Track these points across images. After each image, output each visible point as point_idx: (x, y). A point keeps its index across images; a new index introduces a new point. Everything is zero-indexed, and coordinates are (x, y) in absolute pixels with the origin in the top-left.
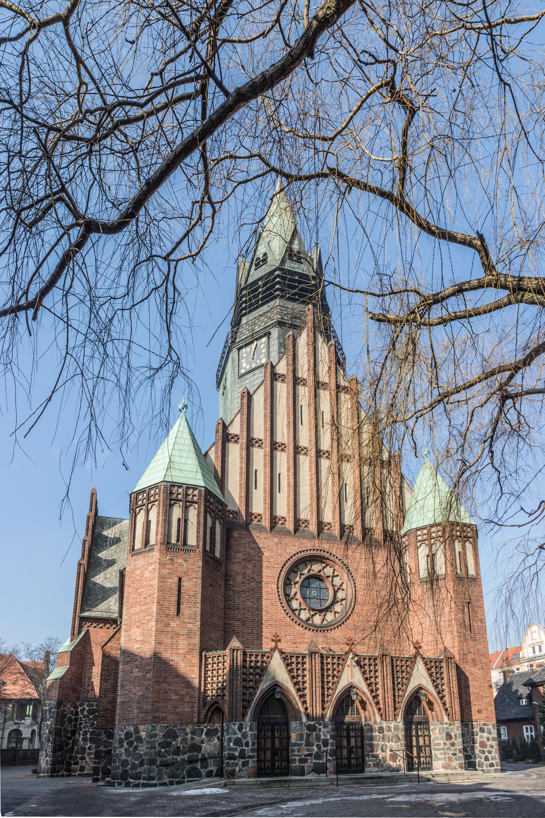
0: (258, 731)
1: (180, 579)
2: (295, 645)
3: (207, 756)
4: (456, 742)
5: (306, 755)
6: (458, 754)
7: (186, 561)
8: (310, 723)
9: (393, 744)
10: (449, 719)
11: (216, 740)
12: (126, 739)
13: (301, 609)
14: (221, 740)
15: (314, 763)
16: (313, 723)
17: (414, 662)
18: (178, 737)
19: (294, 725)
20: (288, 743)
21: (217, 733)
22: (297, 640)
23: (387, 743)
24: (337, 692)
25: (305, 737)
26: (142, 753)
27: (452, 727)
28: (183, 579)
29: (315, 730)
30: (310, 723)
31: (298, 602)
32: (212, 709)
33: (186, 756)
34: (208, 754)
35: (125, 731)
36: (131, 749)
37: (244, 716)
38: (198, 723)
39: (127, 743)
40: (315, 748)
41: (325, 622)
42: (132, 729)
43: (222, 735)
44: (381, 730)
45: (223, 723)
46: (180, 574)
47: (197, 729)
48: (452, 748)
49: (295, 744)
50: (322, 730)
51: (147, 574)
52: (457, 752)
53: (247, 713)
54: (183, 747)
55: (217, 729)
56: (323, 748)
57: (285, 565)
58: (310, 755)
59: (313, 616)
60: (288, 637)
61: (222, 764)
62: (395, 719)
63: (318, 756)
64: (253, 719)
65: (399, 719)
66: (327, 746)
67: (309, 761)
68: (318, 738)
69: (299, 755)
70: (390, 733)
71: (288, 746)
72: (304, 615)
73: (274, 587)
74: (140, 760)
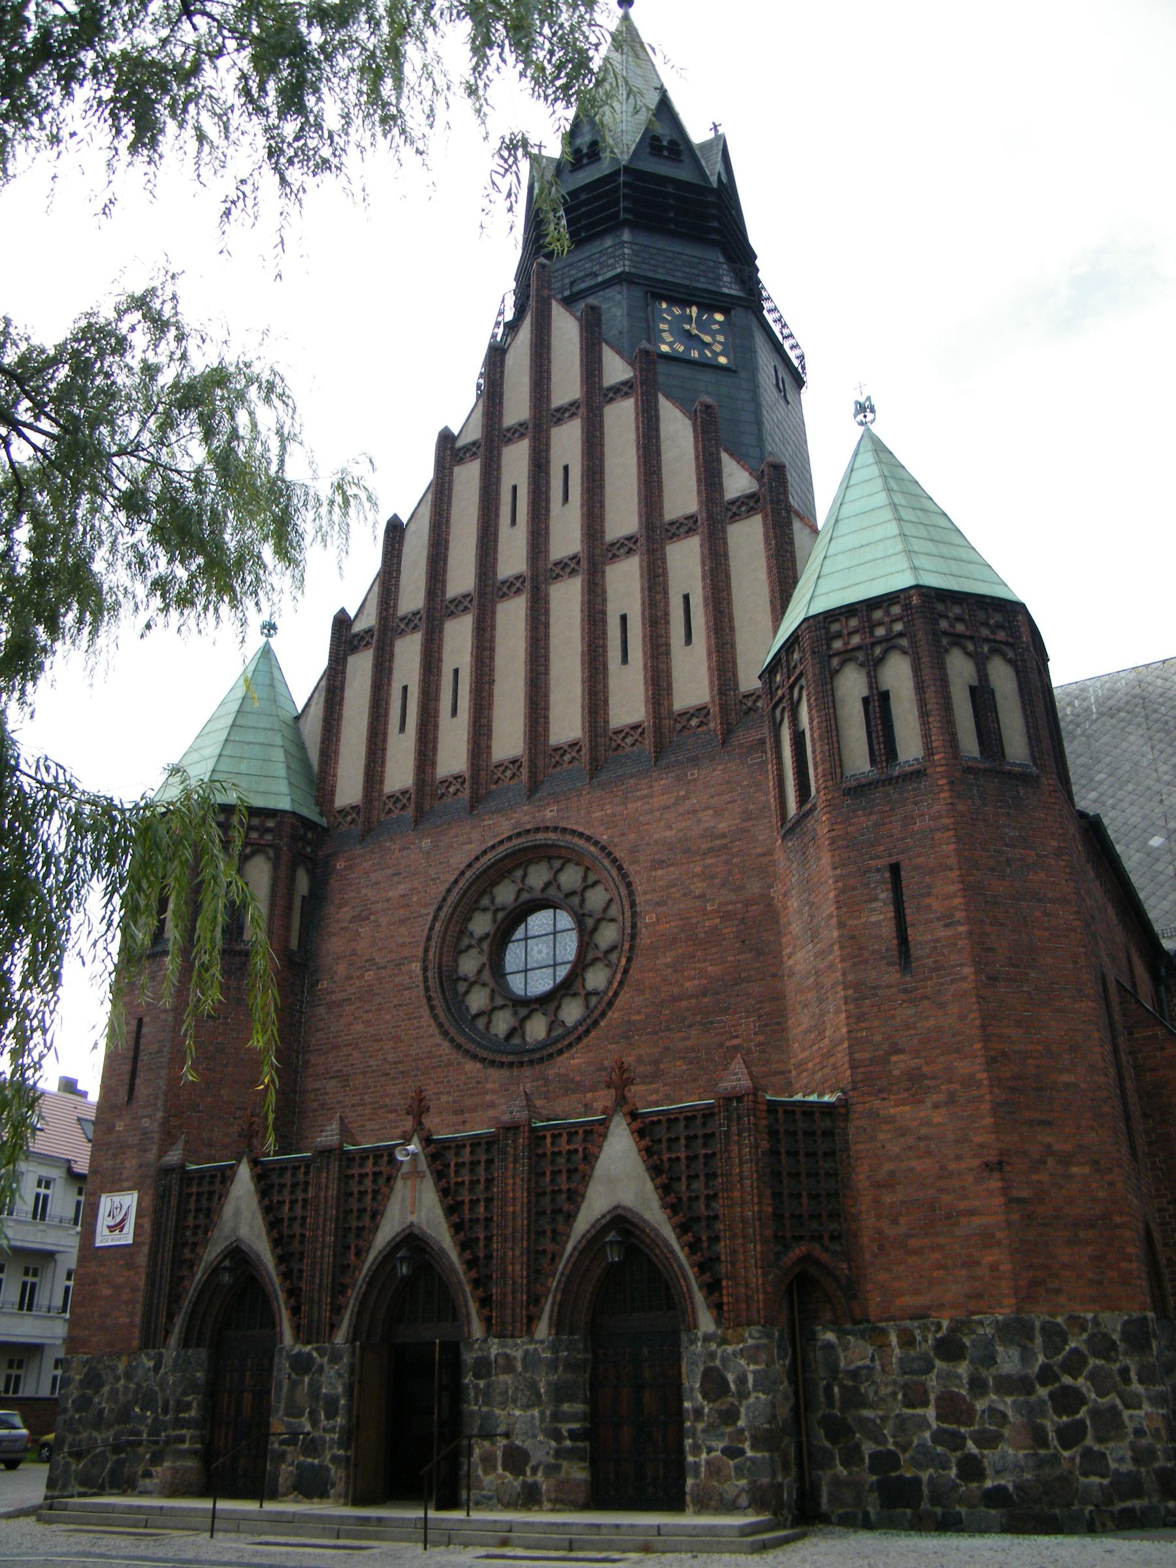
2: (461, 1118)
8: (299, 1348)
9: (517, 1413)
10: (718, 1322)
13: (494, 1009)
15: (300, 1466)
16: (308, 1348)
22: (468, 1102)
23: (497, 1411)
25: (285, 1389)
29: (307, 1371)
30: (299, 1348)
31: (488, 990)
33: (110, 1434)
44: (483, 1367)
50: (326, 1368)
56: (324, 1423)
57: (444, 899)
59: (523, 1021)
60: (444, 1098)
62: (529, 1330)
65: (542, 1330)
67: (289, 1458)
70: (506, 1378)
72: (502, 1023)
73: (416, 967)
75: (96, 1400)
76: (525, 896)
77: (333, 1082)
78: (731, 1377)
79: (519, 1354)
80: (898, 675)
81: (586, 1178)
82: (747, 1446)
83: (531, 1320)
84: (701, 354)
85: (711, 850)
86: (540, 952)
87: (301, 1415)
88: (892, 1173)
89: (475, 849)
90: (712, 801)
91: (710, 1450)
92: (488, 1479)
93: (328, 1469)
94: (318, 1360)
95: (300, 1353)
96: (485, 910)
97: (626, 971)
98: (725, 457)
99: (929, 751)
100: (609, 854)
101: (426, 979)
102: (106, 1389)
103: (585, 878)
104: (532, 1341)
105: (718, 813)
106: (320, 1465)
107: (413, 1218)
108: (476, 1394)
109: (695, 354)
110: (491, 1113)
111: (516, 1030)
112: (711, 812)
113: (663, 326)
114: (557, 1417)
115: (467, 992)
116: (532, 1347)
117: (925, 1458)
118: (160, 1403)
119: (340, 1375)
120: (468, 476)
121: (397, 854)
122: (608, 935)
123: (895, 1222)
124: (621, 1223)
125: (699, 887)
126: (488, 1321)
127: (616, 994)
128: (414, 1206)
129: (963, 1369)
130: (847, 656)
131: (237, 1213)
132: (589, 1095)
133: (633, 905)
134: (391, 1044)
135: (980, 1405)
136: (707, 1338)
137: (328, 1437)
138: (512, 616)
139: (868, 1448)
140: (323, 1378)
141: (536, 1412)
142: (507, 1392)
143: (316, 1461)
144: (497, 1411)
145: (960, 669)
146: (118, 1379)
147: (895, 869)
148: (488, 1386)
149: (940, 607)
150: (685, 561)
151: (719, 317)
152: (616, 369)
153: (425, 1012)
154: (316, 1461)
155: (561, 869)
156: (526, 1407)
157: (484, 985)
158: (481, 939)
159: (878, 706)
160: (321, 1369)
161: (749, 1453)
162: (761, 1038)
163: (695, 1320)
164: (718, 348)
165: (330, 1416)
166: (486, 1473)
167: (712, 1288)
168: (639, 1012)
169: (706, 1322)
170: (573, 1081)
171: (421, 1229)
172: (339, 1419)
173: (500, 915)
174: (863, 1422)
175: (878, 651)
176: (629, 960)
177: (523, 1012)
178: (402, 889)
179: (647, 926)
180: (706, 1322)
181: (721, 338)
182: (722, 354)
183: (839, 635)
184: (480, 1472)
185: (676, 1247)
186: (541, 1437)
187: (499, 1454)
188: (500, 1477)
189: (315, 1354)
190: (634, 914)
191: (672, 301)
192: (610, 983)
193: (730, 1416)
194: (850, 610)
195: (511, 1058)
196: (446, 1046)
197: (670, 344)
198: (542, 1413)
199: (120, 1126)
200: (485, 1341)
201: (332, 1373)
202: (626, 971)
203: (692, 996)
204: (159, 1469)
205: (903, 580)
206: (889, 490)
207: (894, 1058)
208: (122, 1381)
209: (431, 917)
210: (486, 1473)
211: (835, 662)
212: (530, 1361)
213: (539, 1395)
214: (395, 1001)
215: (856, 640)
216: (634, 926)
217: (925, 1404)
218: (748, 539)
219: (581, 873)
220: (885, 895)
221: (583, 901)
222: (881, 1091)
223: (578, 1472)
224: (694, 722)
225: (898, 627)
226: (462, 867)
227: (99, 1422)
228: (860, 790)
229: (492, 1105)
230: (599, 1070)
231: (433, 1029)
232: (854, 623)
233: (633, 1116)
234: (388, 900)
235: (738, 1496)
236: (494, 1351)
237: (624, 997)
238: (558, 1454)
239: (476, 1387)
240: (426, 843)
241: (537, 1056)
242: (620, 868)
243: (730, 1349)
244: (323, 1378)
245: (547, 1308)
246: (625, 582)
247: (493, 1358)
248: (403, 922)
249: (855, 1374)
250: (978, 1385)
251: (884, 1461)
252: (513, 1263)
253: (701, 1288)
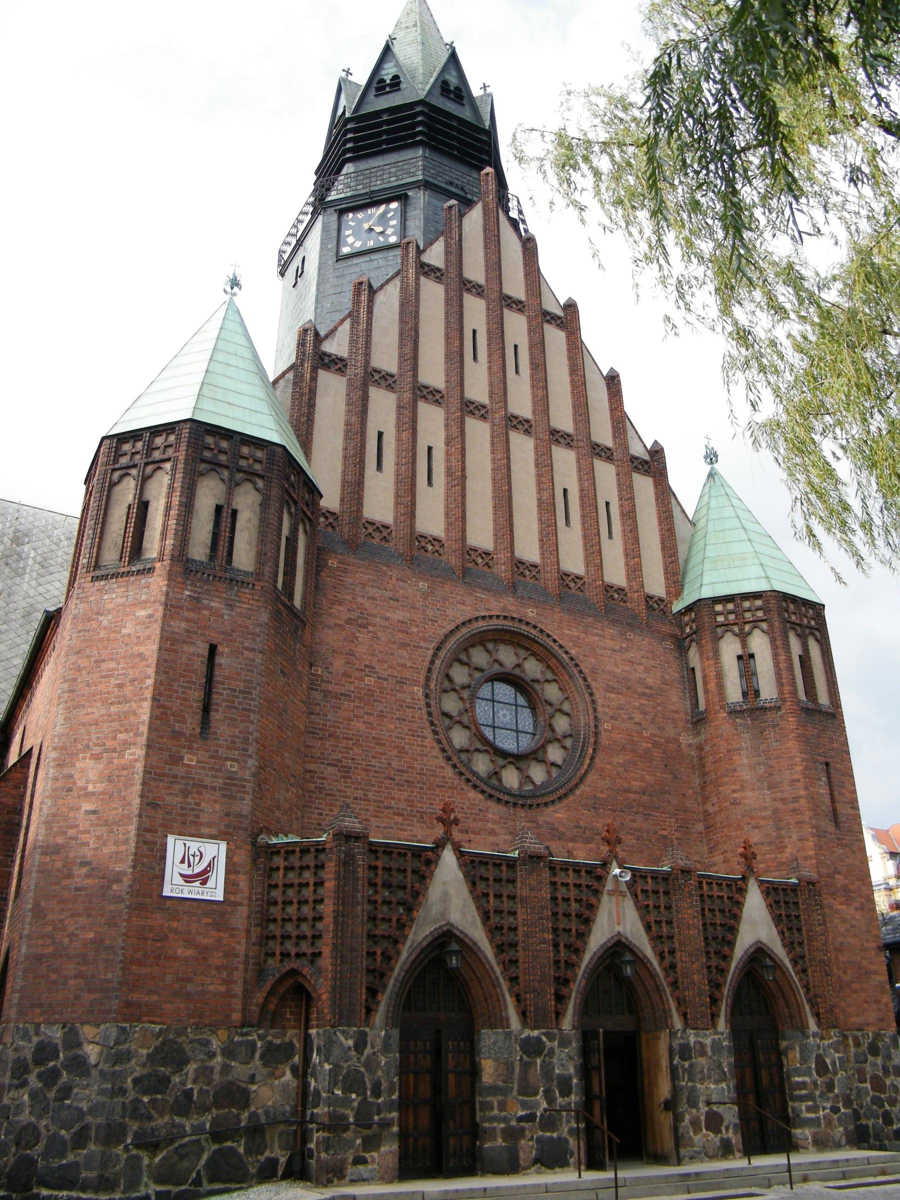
0: (401, 1052)
1: (213, 649)
3: (263, 1120)
5: (521, 1119)
6: (843, 1110)
7: (230, 607)
8: (527, 1033)
9: (712, 1086)
10: (819, 1026)
11: (288, 1076)
12: (38, 1062)
14: (303, 1072)
15: (539, 1140)
16: (535, 1033)
17: (742, 891)
18: (187, 1062)
19: (488, 1038)
20: (473, 1085)
21: (291, 1056)
23: (698, 1086)
24: (587, 957)
25: (517, 1070)
26: (84, 1106)
28: (220, 649)
29: (539, 1053)
30: (527, 1033)
32: (282, 990)
33: (207, 1120)
34: (267, 1113)
35: (35, 1039)
36: (52, 1095)
37: (369, 1011)
38: (243, 1026)
39: (40, 1076)
42: (56, 1034)
43: (307, 1059)
45: (307, 1027)
46: (215, 638)
47: (240, 1044)
49: (493, 1090)
50: (557, 1051)
51: (129, 629)
53: (378, 1003)
54: (201, 1091)
55: (291, 1044)
56: (560, 1100)
58: (530, 1118)
61: (305, 1140)
62: (714, 1026)
63: (549, 1122)
64: (390, 1022)
65: (722, 1024)
66: (568, 1095)
67: (528, 1134)
68: (547, 1071)
69: (505, 1120)
71: (473, 1094)
74: (77, 1127)
75: (176, 1079)
76: (517, 672)
77: (330, 770)
78: (828, 1061)
79: (708, 1042)
82: (841, 1105)
83: (714, 1016)
85: (644, 694)
86: (504, 716)
87: (536, 1093)
88: (842, 943)
89: (468, 612)
90: (643, 661)
91: (824, 1108)
92: (697, 1138)
93: (567, 1141)
94: (548, 1044)
95: (528, 1038)
97: (592, 759)
101: (428, 705)
102: (192, 1067)
104: (716, 1033)
105: (647, 670)
106: (559, 1138)
110: (492, 839)
112: (642, 667)
116: (717, 1037)
118: (369, 1085)
119: (571, 1058)
121: (394, 581)
123: (845, 973)
125: (638, 717)
126: (684, 1015)
127: (586, 773)
128: (617, 919)
129: (879, 1061)
131: (445, 897)
132: (571, 845)
134: (395, 752)
136: (815, 1035)
140: (555, 1060)
141: (724, 1085)
142: (702, 1071)
143: (555, 1135)
144: (698, 1086)
146: (212, 1055)
148: (691, 1066)
153: (428, 733)
154: (555, 1135)
156: (717, 1082)
160: (552, 1051)
162: (679, 835)
165: (566, 1092)
166: (695, 1134)
167: (813, 1004)
168: (602, 792)
169: (813, 1027)
170: (557, 829)
171: (627, 939)
172: (573, 1097)
176: (594, 750)
178: (398, 615)
179: (605, 730)
180: (813, 1027)
184: (691, 1133)
187: (703, 1118)
188: (706, 1136)
189: (544, 1039)
193: (830, 1086)
195: (506, 798)
196: (449, 772)
199: (190, 759)
200: (684, 1031)
201: (563, 1056)
203: (636, 792)
204: (375, 1154)
208: (219, 1059)
209: (430, 653)
210: (695, 1134)
212: (717, 1047)
213: (724, 1073)
214: (398, 714)
217: (866, 1081)
222: (833, 894)
226: (459, 621)
227: (185, 1104)
229: (492, 832)
230: (576, 827)
231: (436, 751)
234: (387, 619)
237: (592, 777)
239: (683, 1066)
240: (423, 585)
241: (529, 802)
242: (585, 679)
243: (826, 1042)
244: (555, 1060)
247: (692, 1044)
248: (404, 645)
252: (695, 974)
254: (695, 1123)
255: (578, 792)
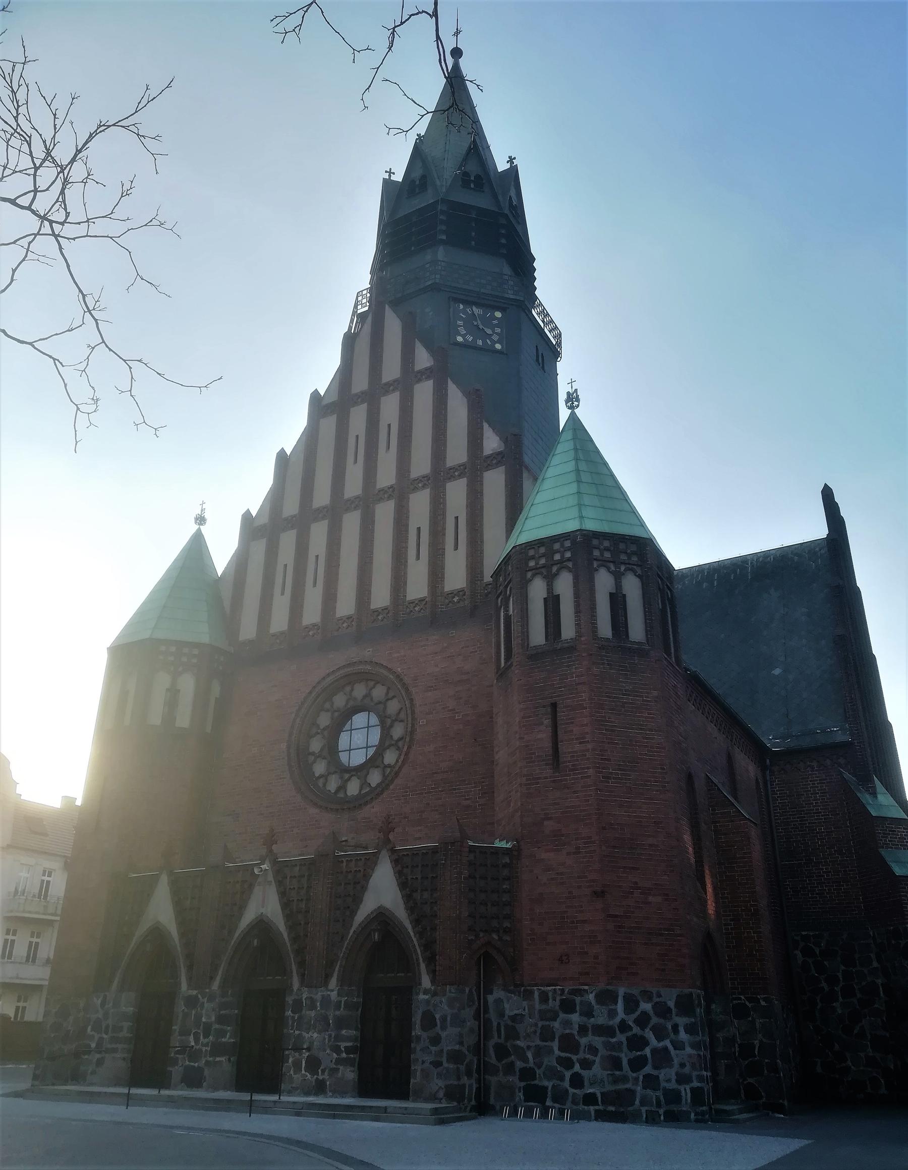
4: (444, 1034)
9: (315, 1035)
10: (433, 982)
23: (304, 1034)
27: (437, 999)
40: (191, 1038)
41: (341, 795)
44: (298, 1006)
48: (433, 1049)
50: (206, 1005)
52: (444, 1060)
65: (333, 983)
67: (180, 1063)
72: (333, 784)
76: (351, 703)
78: (437, 1016)
79: (318, 997)
80: (564, 585)
81: (364, 888)
83: (328, 977)
84: (484, 342)
92: (297, 1078)
96: (328, 711)
97: (407, 754)
98: (486, 425)
99: (579, 634)
100: (401, 680)
103: (387, 694)
106: (199, 1067)
107: (263, 910)
108: (293, 1023)
109: (480, 342)
111: (342, 788)
113: (460, 323)
114: (338, 1038)
115: (314, 762)
117: (552, 1073)
120: (329, 424)
122: (398, 731)
124: (382, 917)
127: (400, 768)
130: (537, 571)
133: (413, 712)
135: (584, 1041)
136: (426, 992)
137: (204, 1049)
138: (352, 522)
139: (519, 1064)
140: (204, 1012)
144: (304, 1034)
145: (604, 581)
147: (554, 706)
148: (300, 1018)
149: (595, 542)
150: (456, 493)
151: (498, 314)
152: (423, 359)
155: (374, 687)
157: (324, 758)
158: (324, 729)
159: (552, 603)
161: (445, 1064)
163: (420, 979)
164: (495, 338)
165: (206, 1036)
167: (431, 960)
172: (211, 1038)
173: (336, 714)
174: (516, 1047)
175: (555, 569)
176: (409, 747)
177: (347, 776)
181: (498, 330)
182: (499, 342)
183: (533, 558)
184: (292, 1072)
185: (412, 934)
186: (328, 1051)
190: (413, 719)
191: (467, 303)
192: (397, 761)
194: (541, 542)
197: (463, 336)
198: (330, 1036)
202: (407, 754)
205: (572, 526)
206: (577, 459)
207: (546, 823)
211: (529, 574)
215: (543, 561)
216: (413, 725)
218: (495, 482)
219: (385, 691)
220: (547, 722)
221: (385, 708)
223: (349, 1074)
224: (455, 599)
225: (568, 555)
228: (536, 656)
232: (542, 550)
233: (393, 851)
235: (438, 1091)
236: (304, 996)
238: (339, 1061)
242: (407, 690)
245: (337, 969)
246: (420, 504)
249: (514, 1018)
250: (583, 1030)
251: (527, 1074)
253: (424, 961)
254: (297, 1065)
255: (391, 787)
